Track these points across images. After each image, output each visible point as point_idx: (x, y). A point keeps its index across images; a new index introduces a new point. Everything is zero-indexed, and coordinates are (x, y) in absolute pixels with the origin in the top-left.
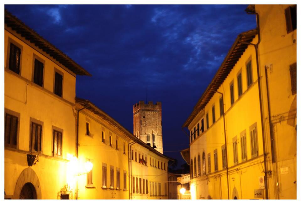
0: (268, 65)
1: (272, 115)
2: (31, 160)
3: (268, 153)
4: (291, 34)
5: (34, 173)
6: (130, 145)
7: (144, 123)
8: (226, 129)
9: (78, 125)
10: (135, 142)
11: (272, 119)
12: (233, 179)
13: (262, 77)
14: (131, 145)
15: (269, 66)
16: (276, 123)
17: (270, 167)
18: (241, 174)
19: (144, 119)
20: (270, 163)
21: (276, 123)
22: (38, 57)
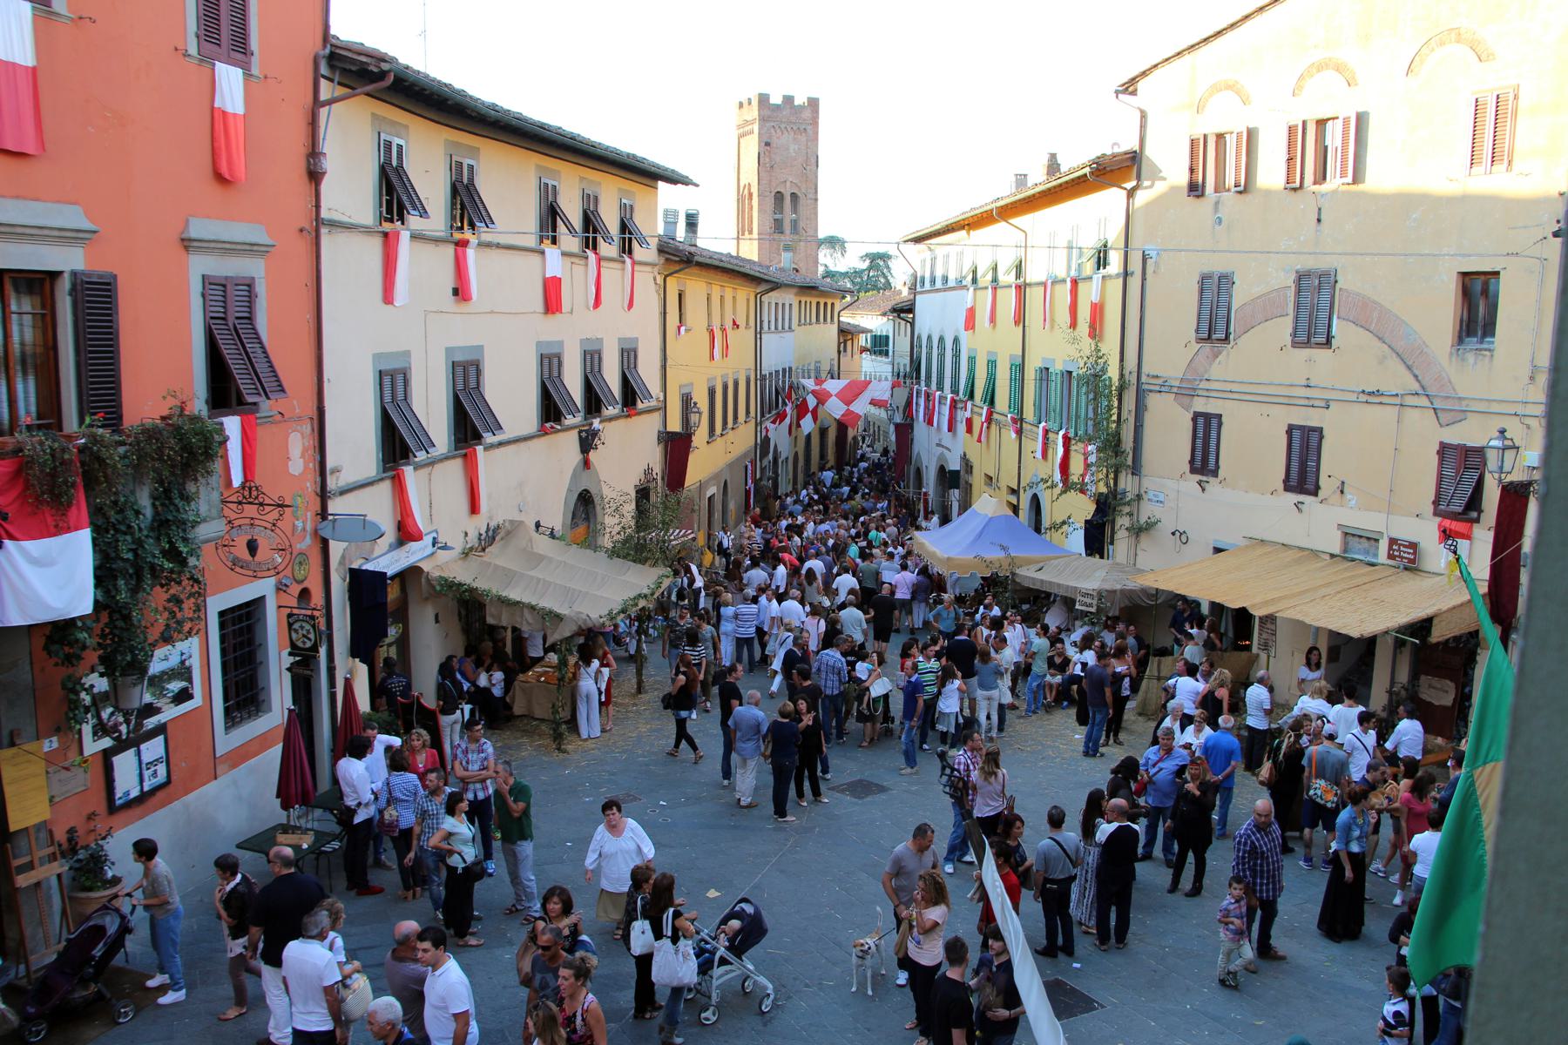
0: (1152, 249)
1: (1145, 369)
2: (587, 443)
7: (767, 160)
9: (665, 313)
11: (1144, 379)
13: (1132, 273)
15: (1153, 254)
16: (1151, 391)
17: (1127, 483)
21: (1151, 391)
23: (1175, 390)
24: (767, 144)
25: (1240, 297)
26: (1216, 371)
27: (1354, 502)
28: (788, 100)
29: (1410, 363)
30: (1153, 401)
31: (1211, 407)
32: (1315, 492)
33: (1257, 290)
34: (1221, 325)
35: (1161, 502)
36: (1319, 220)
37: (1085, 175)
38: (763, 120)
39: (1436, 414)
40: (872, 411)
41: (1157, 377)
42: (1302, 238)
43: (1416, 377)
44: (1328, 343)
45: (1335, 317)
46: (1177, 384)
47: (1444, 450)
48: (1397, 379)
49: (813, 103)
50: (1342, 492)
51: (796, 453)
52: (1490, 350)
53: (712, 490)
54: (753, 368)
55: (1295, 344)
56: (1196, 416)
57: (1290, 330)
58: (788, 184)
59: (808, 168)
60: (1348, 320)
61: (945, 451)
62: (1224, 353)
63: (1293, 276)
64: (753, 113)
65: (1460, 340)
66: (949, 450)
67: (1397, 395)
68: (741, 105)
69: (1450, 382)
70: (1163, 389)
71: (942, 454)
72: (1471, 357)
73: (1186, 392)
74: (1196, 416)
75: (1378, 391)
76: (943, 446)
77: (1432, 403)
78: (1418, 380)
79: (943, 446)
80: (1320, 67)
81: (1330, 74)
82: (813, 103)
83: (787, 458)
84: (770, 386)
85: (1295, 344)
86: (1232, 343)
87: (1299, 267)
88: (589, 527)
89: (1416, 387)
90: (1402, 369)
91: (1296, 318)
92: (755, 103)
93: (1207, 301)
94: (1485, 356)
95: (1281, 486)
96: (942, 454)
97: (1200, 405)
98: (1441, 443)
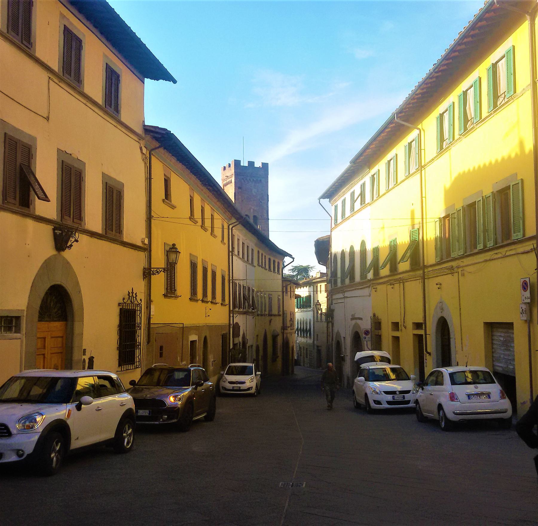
5: (67, 265)
6: (231, 227)
7: (240, 197)
8: (424, 196)
9: (150, 179)
10: (238, 223)
12: (438, 286)
14: (232, 228)
18: (463, 275)
19: (240, 190)
22: (71, 24)
24: (240, 188)
28: (251, 164)
38: (237, 174)
40: (302, 341)
49: (265, 166)
51: (258, 347)
53: (193, 337)
54: (227, 273)
58: (252, 210)
59: (263, 202)
61: (359, 322)
64: (232, 171)
66: (361, 319)
68: (225, 168)
71: (356, 324)
76: (356, 319)
79: (356, 319)
82: (265, 166)
83: (252, 346)
84: (240, 294)
88: (66, 325)
92: (233, 166)
96: (356, 324)
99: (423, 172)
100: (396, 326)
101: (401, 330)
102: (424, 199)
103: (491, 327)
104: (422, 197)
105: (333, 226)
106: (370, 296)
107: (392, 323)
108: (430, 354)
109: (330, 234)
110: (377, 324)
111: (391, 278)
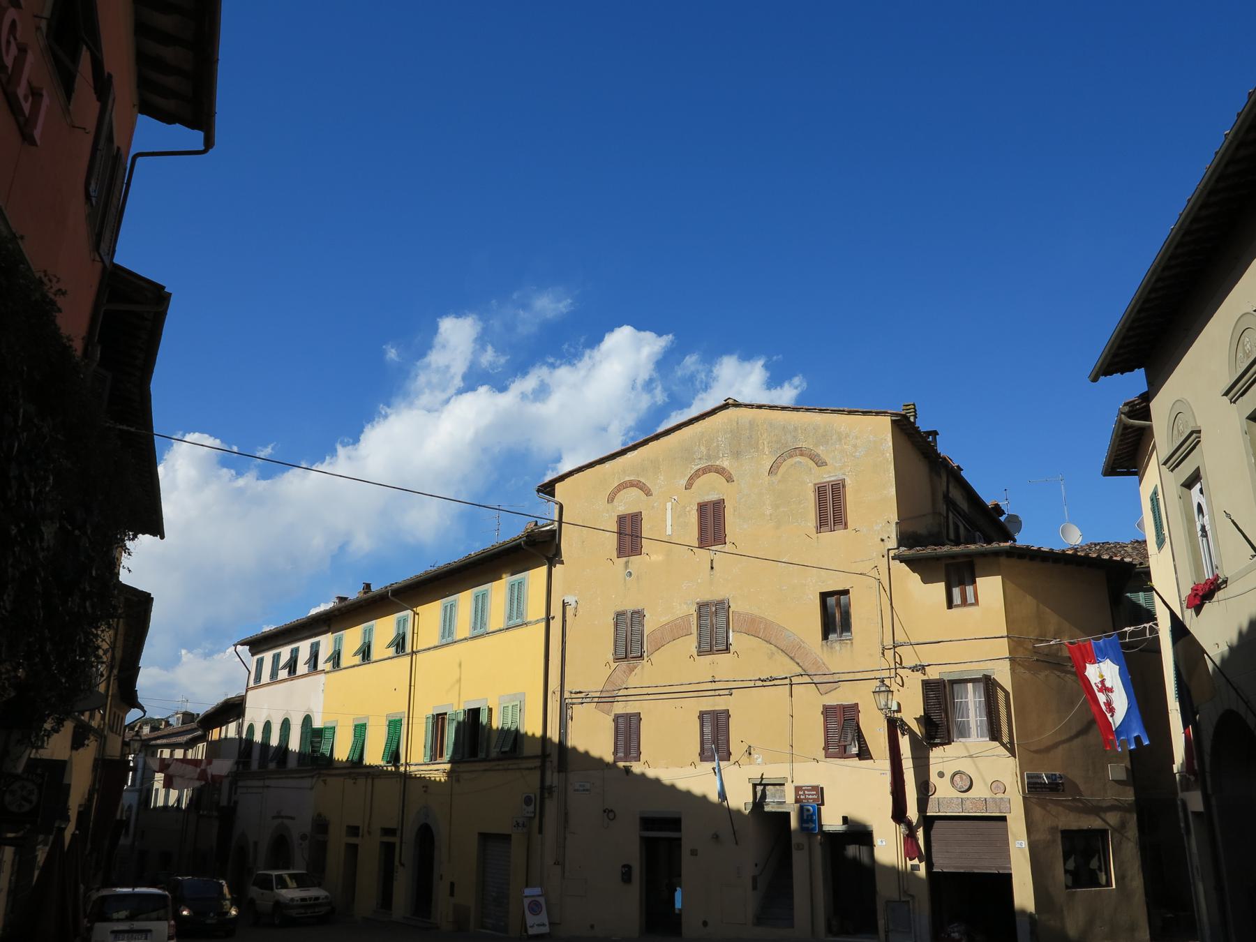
0: (570, 599)
3: (549, 755)
4: (624, 559)
11: (566, 695)
12: (424, 789)
13: (553, 618)
16: (573, 704)
17: (552, 778)
20: (553, 772)
21: (573, 704)
23: (596, 700)
25: (650, 625)
26: (633, 681)
27: (760, 760)
29: (792, 656)
30: (577, 711)
31: (631, 708)
32: (727, 756)
33: (664, 619)
34: (636, 647)
35: (587, 790)
36: (712, 568)
37: (520, 544)
39: (817, 687)
41: (580, 692)
42: (699, 581)
43: (798, 664)
44: (727, 650)
45: (731, 631)
46: (598, 694)
47: (828, 711)
48: (784, 667)
50: (750, 754)
52: (850, 640)
55: (700, 653)
56: (617, 718)
57: (695, 644)
60: (741, 632)
61: (286, 821)
62: (640, 667)
63: (695, 607)
65: (825, 637)
67: (786, 678)
69: (824, 665)
70: (584, 700)
72: (837, 646)
73: (605, 699)
74: (617, 718)
75: (771, 677)
76: (282, 817)
77: (812, 680)
78: (800, 666)
79: (282, 817)
80: (705, 470)
81: (713, 476)
85: (700, 653)
86: (646, 659)
87: (698, 600)
89: (799, 671)
90: (787, 660)
91: (700, 635)
93: (622, 634)
94: (847, 643)
95: (698, 758)
97: (620, 708)
98: (824, 706)
99: (414, 656)
100: (354, 831)
101: (363, 836)
102: (412, 688)
103: (485, 838)
104: (410, 686)
105: (252, 684)
106: (312, 789)
107: (348, 827)
108: (402, 865)
109: (244, 694)
110: (321, 826)
111: (352, 771)
